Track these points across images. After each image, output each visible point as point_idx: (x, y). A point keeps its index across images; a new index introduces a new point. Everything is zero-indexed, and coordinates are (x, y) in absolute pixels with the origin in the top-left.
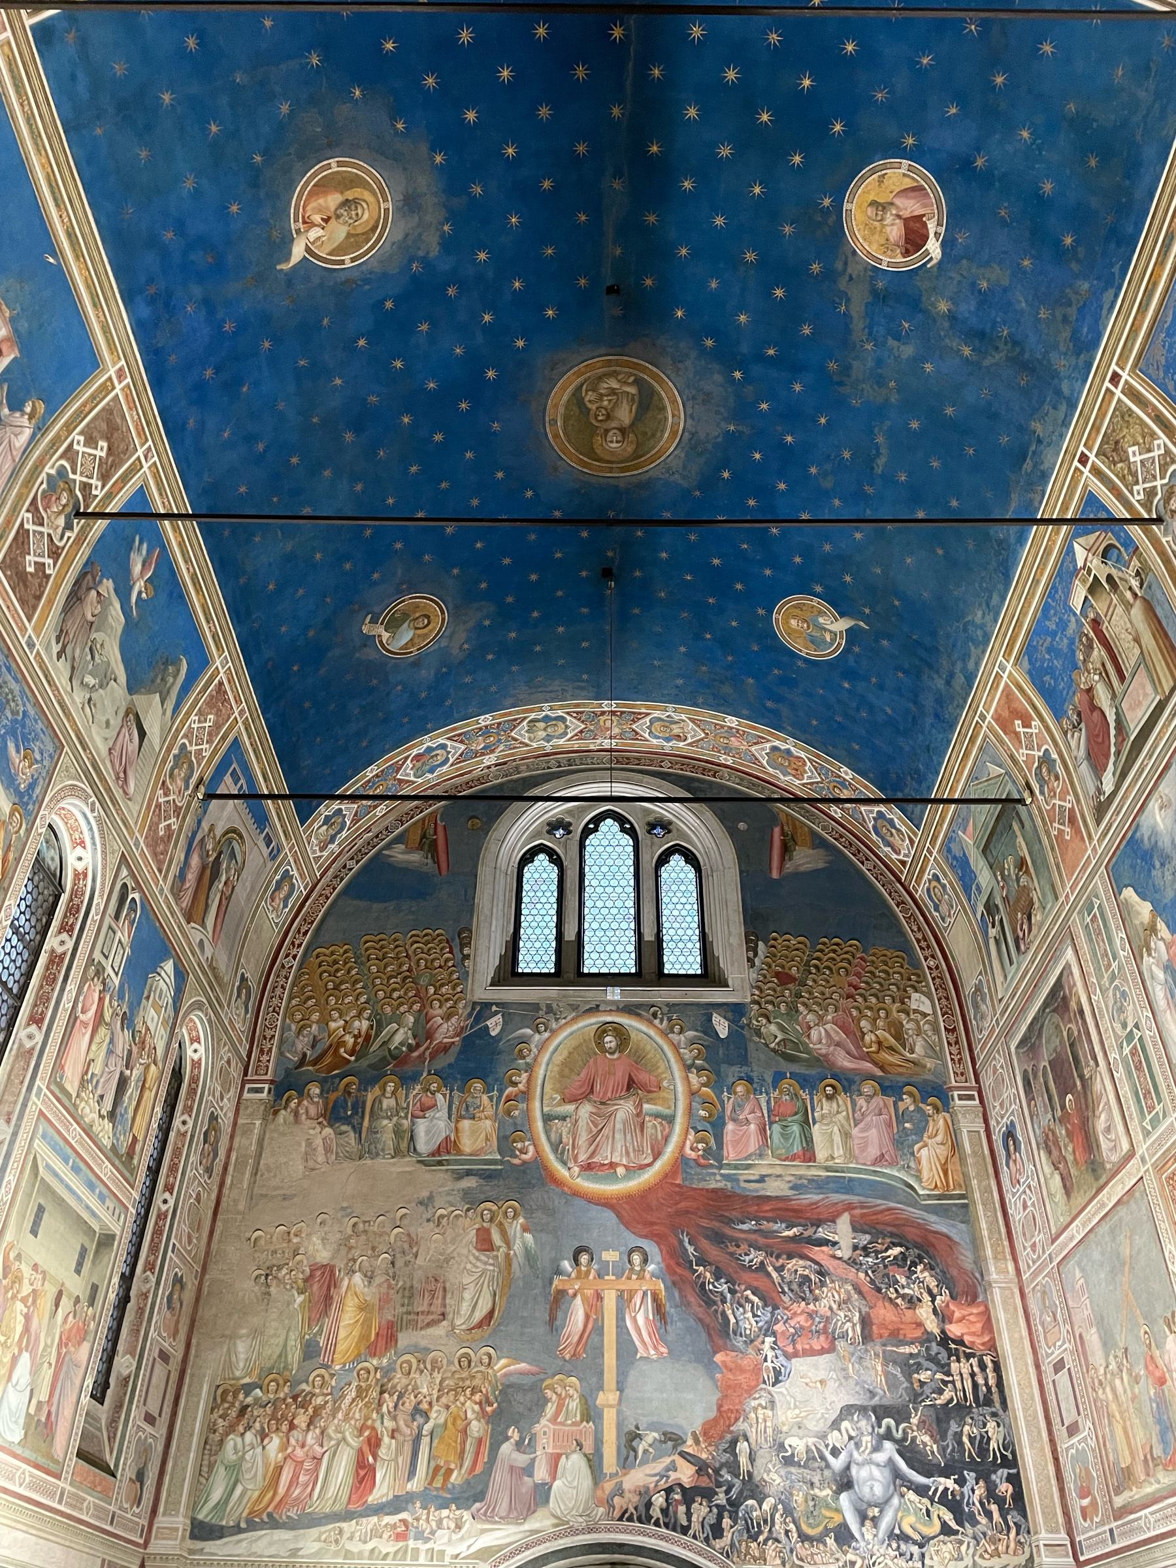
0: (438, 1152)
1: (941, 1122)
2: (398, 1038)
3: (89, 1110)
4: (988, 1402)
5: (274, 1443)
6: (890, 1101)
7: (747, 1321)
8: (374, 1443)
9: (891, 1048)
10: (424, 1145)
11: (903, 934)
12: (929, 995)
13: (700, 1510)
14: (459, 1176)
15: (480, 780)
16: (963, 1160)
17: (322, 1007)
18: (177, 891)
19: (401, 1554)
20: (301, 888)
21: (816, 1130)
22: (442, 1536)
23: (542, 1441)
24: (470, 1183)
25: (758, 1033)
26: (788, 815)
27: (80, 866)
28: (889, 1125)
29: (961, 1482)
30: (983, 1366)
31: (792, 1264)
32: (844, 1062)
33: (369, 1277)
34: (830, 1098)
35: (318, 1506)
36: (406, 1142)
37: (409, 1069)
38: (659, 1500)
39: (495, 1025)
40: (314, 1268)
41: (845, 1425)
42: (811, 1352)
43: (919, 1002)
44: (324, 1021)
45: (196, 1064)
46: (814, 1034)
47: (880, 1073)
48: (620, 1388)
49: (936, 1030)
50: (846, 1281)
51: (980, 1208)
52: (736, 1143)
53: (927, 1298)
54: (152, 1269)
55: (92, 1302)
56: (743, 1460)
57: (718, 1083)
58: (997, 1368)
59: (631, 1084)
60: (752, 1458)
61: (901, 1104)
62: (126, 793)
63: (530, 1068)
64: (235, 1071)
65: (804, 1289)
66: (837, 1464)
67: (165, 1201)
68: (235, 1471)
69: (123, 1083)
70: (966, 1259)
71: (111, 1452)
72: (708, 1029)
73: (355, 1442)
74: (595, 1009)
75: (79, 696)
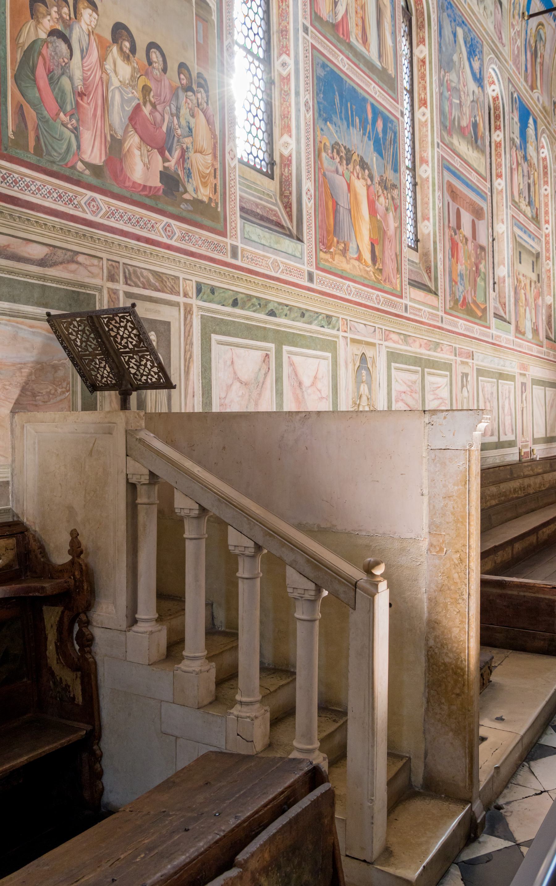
3: (523, 205)
18: (526, 81)
27: (494, 94)
45: (544, 159)
54: (549, 259)
55: (539, 282)
62: (503, 44)
67: (547, 229)
71: (551, 333)
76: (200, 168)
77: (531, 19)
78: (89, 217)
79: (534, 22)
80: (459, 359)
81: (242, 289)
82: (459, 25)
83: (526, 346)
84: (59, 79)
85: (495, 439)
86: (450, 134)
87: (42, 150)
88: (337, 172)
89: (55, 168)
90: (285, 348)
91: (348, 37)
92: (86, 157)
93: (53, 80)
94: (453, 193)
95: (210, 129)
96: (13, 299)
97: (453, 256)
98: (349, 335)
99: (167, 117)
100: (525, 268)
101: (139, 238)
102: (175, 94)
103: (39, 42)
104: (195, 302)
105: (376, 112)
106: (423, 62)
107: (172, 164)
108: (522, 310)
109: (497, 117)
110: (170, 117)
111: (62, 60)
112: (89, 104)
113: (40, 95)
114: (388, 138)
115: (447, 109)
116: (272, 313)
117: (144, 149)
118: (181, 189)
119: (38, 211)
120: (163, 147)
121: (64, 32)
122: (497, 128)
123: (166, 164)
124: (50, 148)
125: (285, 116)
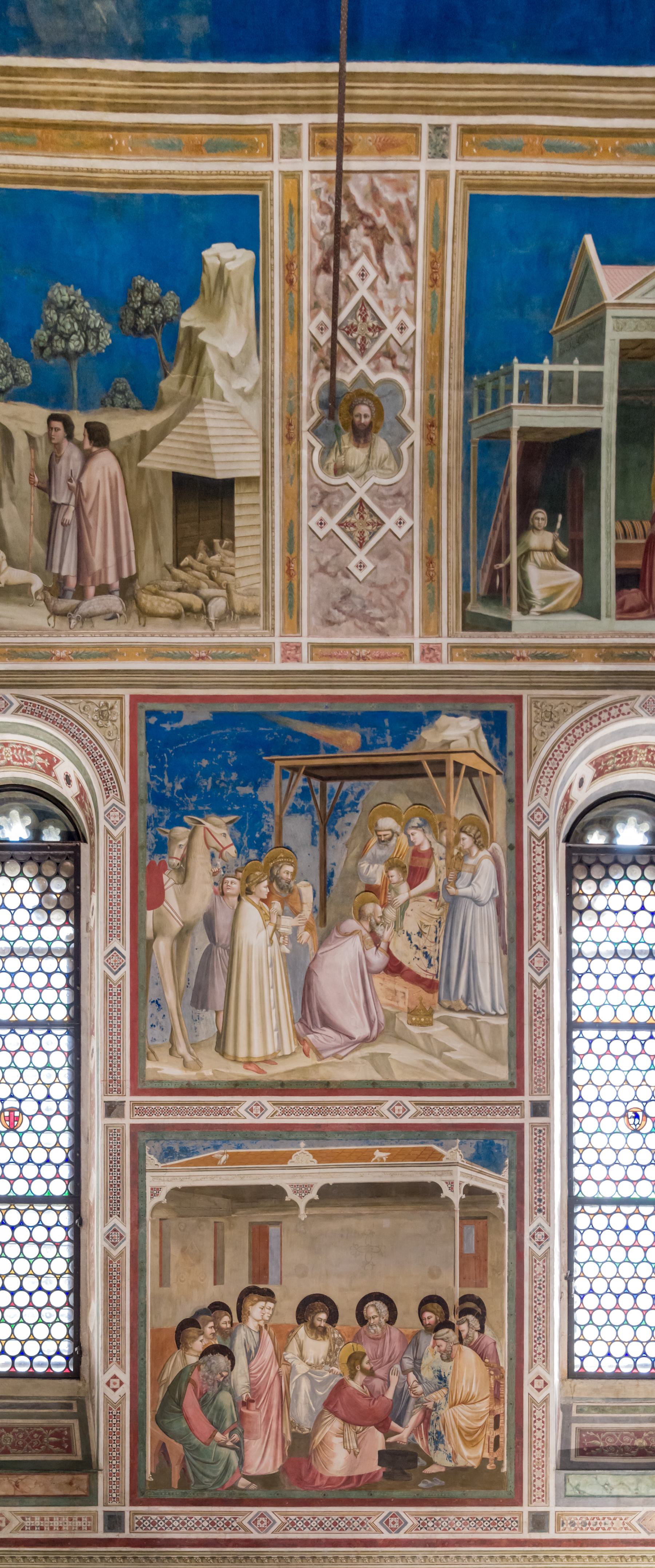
76: (463, 1424)
78: (255, 1535)
84: (214, 1398)
87: (189, 1481)
89: (206, 1495)
92: (252, 1471)
95: (487, 1365)
99: (394, 1380)
102: (412, 1343)
103: (189, 1369)
107: (403, 1434)
110: (402, 1376)
111: (219, 1376)
112: (258, 1409)
113: (188, 1424)
117: (350, 1432)
118: (421, 1462)
119: (181, 1546)
120: (387, 1418)
121: (223, 1344)
123: (391, 1439)
124: (200, 1475)
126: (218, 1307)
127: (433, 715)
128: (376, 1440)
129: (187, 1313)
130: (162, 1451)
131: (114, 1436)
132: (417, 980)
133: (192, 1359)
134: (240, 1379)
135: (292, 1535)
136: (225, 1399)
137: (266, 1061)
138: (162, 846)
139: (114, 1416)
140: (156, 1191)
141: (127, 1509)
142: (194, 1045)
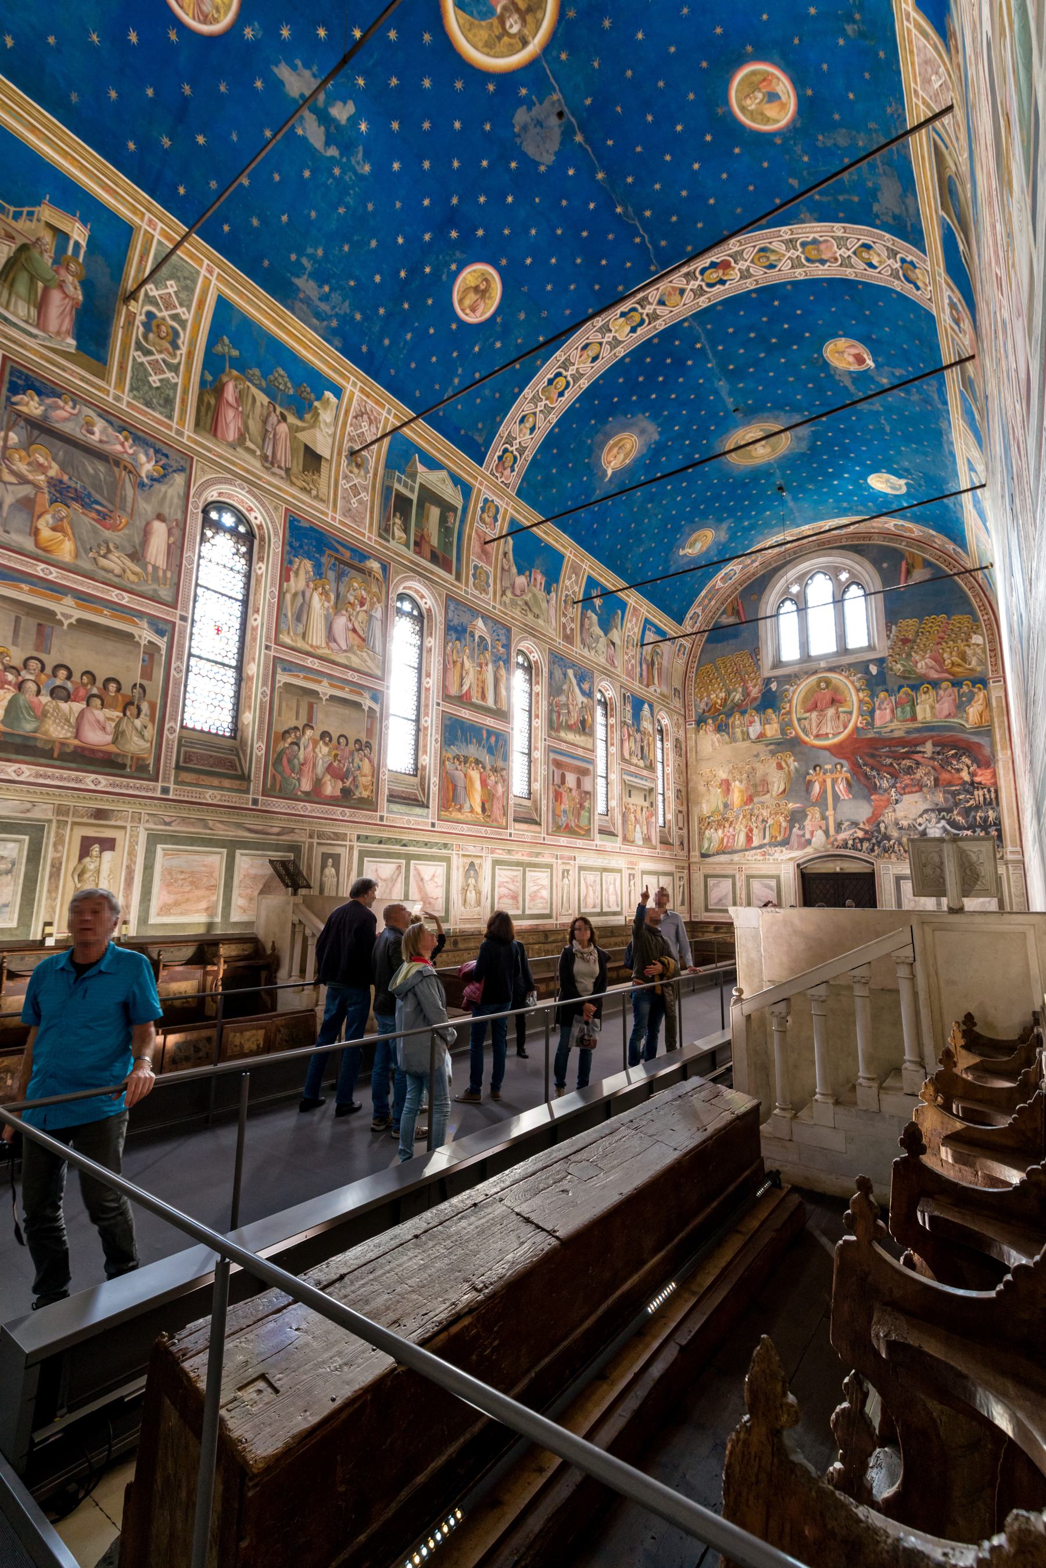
0: (758, 738)
1: (981, 695)
2: (737, 697)
3: (635, 760)
4: (990, 803)
5: (720, 832)
6: (956, 690)
7: (885, 784)
8: (751, 830)
9: (959, 665)
10: (753, 736)
11: (970, 605)
12: (982, 635)
13: (866, 845)
14: (767, 745)
15: (754, 574)
16: (991, 711)
17: (707, 690)
18: (641, 682)
19: (764, 860)
20: (688, 645)
21: (918, 708)
22: (776, 856)
23: (807, 827)
24: (772, 747)
25: (892, 670)
26: (910, 552)
28: (954, 700)
29: (974, 832)
30: (989, 791)
31: (904, 762)
32: (934, 675)
33: (741, 781)
34: (925, 693)
35: (736, 848)
36: (746, 736)
37: (743, 709)
38: (850, 842)
39: (774, 686)
40: (722, 781)
41: (925, 816)
42: (912, 792)
43: (977, 639)
44: (708, 696)
46: (919, 665)
47: (951, 677)
48: (834, 809)
49: (984, 652)
50: (927, 766)
51: (997, 730)
52: (881, 718)
53: (966, 768)
56: (883, 829)
57: (873, 695)
58: (996, 791)
59: (833, 702)
60: (886, 828)
61: (962, 691)
63: (790, 701)
64: (681, 721)
65: (909, 771)
66: (920, 828)
68: (710, 840)
69: (642, 748)
70: (987, 751)
72: (867, 671)
73: (745, 830)
74: (815, 672)
75: (593, 652)
77: (645, 647)
79: (650, 647)
80: (560, 861)
81: (385, 835)
82: (569, 668)
83: (634, 850)
85: (598, 910)
86: (557, 730)
88: (457, 769)
90: (412, 862)
91: (470, 699)
93: (290, 761)
94: (558, 764)
96: (263, 850)
97: (556, 800)
98: (461, 853)
100: (637, 800)
101: (326, 819)
102: (352, 753)
104: (355, 844)
105: (490, 733)
106: (538, 694)
107: (348, 784)
108: (631, 827)
109: (612, 710)
114: (500, 744)
115: (555, 718)
116: (405, 845)
122: (612, 716)
125: (425, 746)
126: (296, 728)
127: (369, 558)
128: (340, 785)
129: (286, 728)
130: (274, 777)
131: (258, 769)
132: (360, 637)
133: (287, 745)
134: (301, 755)
135: (314, 814)
136: (296, 761)
137: (318, 647)
138: (291, 562)
139: (258, 761)
140: (279, 681)
141: (260, 798)
142: (295, 634)
